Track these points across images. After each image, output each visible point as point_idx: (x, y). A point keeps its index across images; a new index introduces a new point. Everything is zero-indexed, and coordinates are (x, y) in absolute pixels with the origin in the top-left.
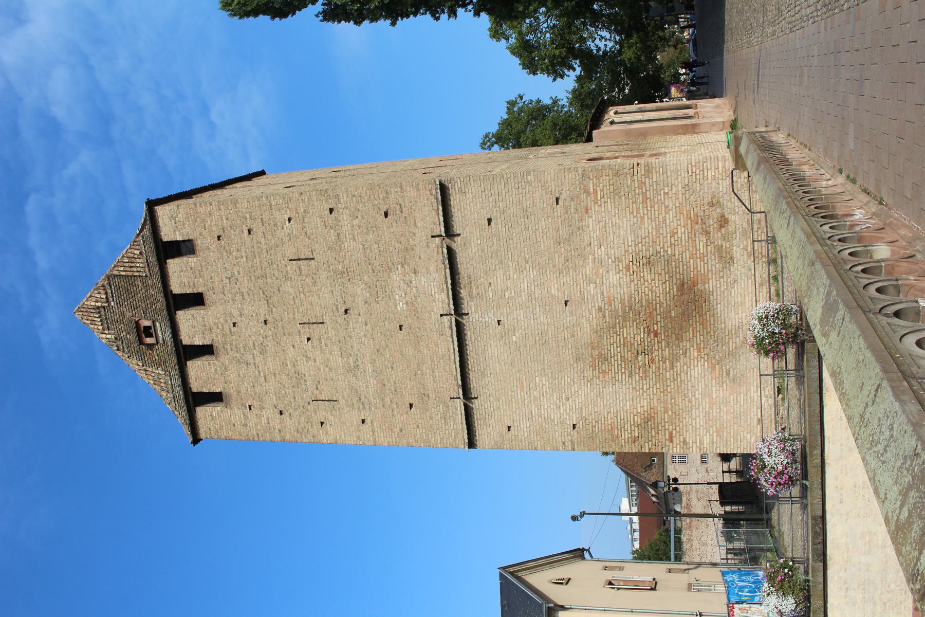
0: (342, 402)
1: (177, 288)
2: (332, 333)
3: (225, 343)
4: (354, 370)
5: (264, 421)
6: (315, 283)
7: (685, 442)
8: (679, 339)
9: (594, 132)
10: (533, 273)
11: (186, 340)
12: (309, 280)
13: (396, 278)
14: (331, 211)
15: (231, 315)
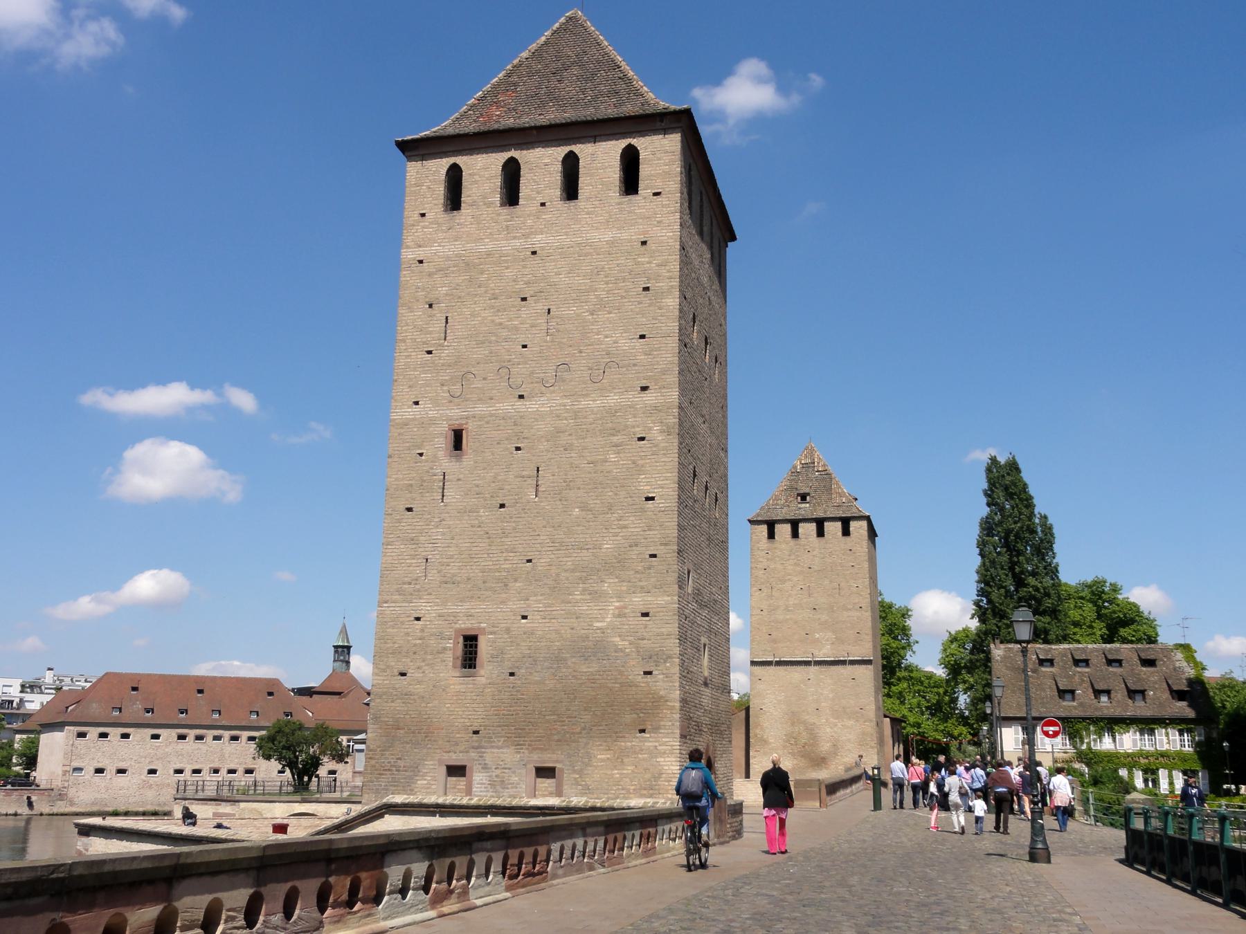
0: (772, 602)
1: (826, 524)
2: (805, 600)
3: (800, 545)
4: (787, 609)
5: (761, 559)
6: (828, 595)
7: (755, 757)
8: (802, 756)
9: (888, 719)
10: (831, 696)
11: (801, 525)
12: (830, 593)
13: (830, 635)
14: (861, 607)
15: (813, 551)
